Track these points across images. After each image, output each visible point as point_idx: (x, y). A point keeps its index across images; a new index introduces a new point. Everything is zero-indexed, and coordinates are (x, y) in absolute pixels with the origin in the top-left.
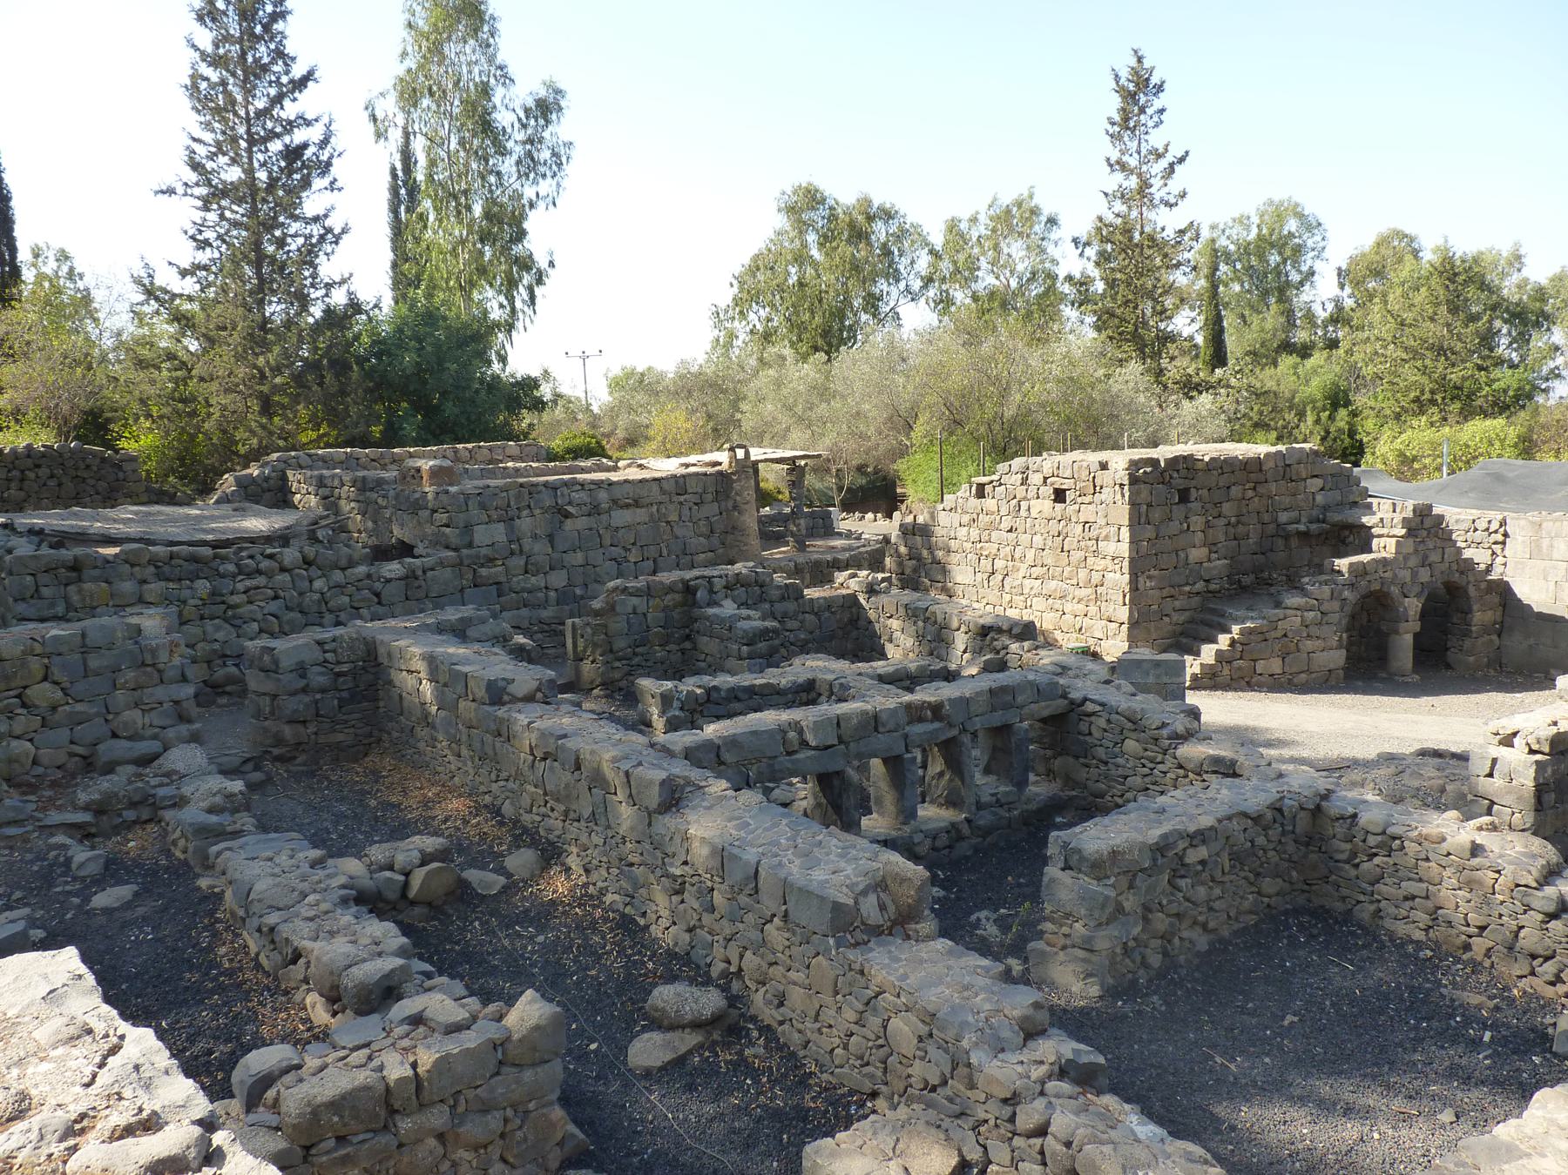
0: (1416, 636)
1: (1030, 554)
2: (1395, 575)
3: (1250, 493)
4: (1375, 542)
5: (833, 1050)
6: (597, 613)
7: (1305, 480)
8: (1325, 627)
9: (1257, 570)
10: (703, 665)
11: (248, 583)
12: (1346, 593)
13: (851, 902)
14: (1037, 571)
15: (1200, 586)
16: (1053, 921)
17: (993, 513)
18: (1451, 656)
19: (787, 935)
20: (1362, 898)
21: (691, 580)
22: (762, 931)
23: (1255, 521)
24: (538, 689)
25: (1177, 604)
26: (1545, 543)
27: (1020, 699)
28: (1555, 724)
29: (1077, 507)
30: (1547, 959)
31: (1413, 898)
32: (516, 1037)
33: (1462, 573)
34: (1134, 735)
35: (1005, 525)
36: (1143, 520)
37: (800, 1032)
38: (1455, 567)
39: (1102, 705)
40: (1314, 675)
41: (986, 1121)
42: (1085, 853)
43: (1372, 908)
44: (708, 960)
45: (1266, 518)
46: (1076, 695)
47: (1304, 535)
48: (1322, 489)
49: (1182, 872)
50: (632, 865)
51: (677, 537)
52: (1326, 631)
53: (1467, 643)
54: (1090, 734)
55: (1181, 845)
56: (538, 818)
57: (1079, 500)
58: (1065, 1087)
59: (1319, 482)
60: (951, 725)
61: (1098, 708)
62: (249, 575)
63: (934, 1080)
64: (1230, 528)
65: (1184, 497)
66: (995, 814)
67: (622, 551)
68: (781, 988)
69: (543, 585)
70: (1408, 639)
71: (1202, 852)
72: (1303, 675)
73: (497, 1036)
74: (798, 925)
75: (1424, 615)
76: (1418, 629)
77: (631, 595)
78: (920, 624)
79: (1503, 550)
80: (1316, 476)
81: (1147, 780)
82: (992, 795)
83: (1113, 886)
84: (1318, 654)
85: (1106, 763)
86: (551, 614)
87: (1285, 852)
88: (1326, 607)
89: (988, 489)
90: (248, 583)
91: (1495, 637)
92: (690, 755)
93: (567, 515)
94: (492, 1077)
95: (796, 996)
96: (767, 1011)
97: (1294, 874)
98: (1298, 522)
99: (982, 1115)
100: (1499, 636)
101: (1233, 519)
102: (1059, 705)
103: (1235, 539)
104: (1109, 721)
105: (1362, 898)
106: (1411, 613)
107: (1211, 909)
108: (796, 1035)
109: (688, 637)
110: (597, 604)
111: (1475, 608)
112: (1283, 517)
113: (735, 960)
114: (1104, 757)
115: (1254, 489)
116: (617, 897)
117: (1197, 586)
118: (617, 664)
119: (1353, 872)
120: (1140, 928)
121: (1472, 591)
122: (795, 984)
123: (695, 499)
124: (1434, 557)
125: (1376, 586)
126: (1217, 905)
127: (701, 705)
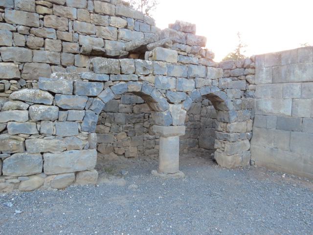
2: (157, 79)
4: (147, 53)
12: (94, 91)
18: (217, 155)
33: (223, 90)
38: (216, 83)
40: (50, 178)
45: (65, 36)
48: (126, 27)
52: (65, 128)
53: (228, 146)
59: (123, 22)
72: (35, 178)
76: (183, 133)
79: (254, 78)
80: (121, 16)
88: (62, 101)
91: (247, 142)
100: (250, 141)
103: (26, 46)
111: (233, 118)
115: (52, 7)
121: (231, 106)
125: (135, 87)
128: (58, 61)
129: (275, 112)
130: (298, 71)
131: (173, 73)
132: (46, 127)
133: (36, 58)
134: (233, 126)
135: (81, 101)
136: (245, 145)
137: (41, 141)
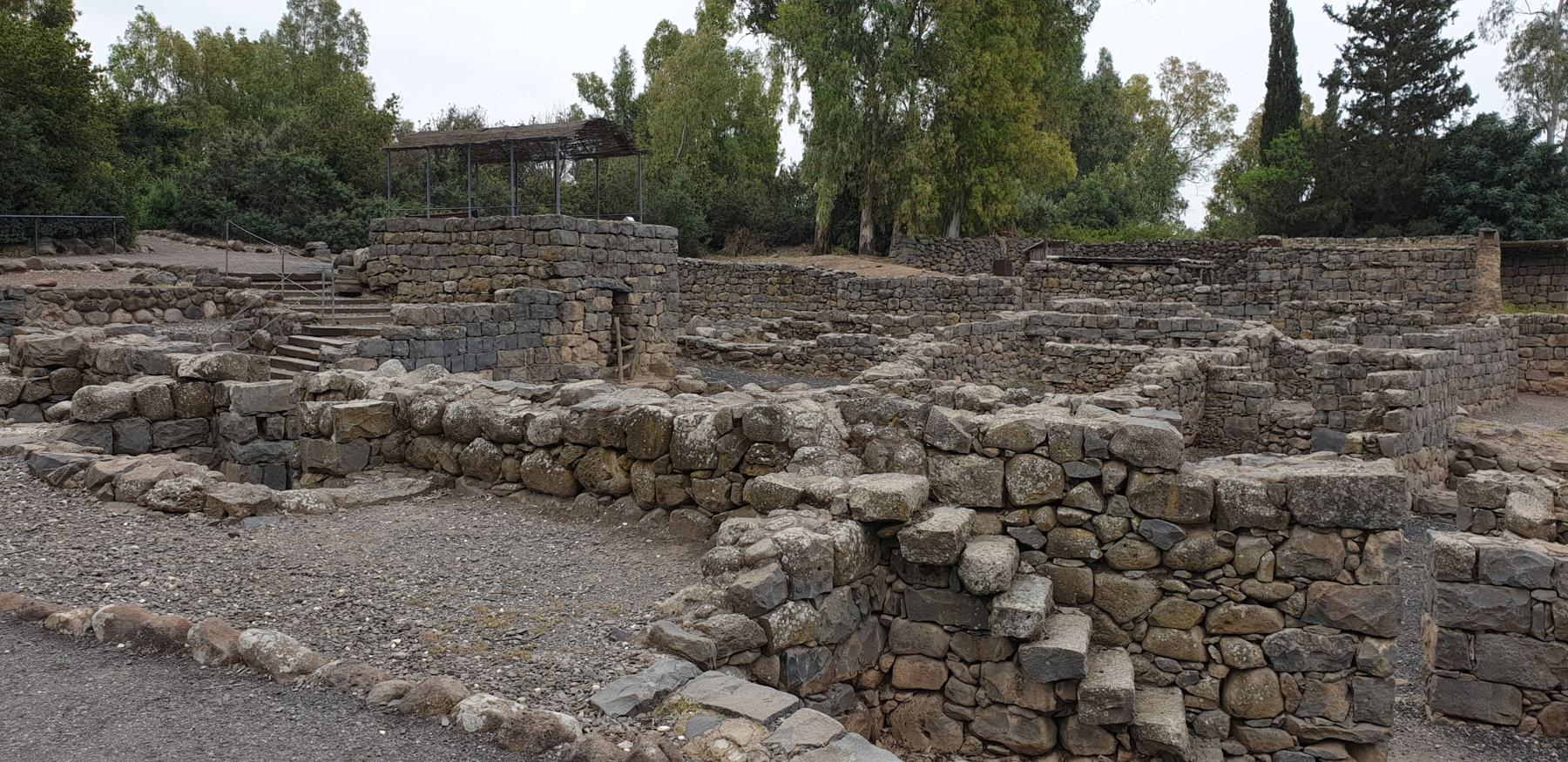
11: (1121, 286)
51: (1420, 290)
55: (1088, 353)
62: (1123, 282)
90: (1121, 286)
93: (1325, 269)
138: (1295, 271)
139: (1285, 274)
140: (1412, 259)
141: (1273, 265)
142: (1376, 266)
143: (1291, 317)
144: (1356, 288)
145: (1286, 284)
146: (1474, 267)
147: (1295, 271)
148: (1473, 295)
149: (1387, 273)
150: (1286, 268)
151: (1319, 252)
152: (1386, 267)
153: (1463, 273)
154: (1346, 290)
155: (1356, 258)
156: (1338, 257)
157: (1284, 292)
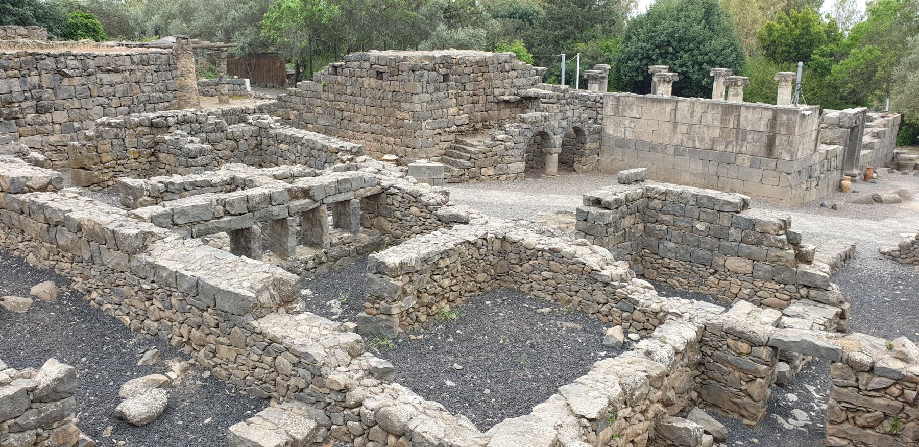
0: (560, 155)
1: (364, 109)
3: (480, 78)
5: (245, 377)
6: (89, 139)
7: (508, 72)
8: (515, 151)
9: (484, 120)
10: (163, 171)
13: (254, 295)
14: (367, 118)
15: (454, 128)
16: (369, 301)
17: (342, 84)
19: (216, 317)
20: (524, 281)
21: (154, 118)
22: (202, 316)
23: (482, 94)
24: (50, 183)
25: (442, 138)
26: (621, 108)
27: (354, 186)
28: (615, 194)
29: (389, 82)
30: (605, 304)
31: (547, 279)
32: (41, 387)
34: (414, 204)
35: (349, 92)
36: (424, 91)
37: (225, 369)
39: (399, 189)
41: (330, 403)
42: (387, 264)
43: (528, 286)
44: (170, 336)
45: (488, 91)
46: (385, 183)
47: (507, 102)
49: (437, 272)
50: (119, 285)
51: (143, 92)
53: (583, 159)
54: (393, 204)
55: (437, 258)
56: (53, 263)
57: (390, 79)
58: (373, 381)
59: (515, 73)
60: (315, 201)
61: (396, 191)
63: (301, 386)
64: (469, 97)
65: (446, 77)
66: (341, 248)
67: (106, 100)
68: (214, 347)
69: (50, 120)
70: (556, 156)
71: (448, 261)
73: (29, 386)
74: (223, 311)
75: (563, 145)
77: (113, 127)
78: (299, 146)
81: (422, 227)
82: (339, 239)
83: (401, 280)
84: (512, 164)
85: (401, 220)
86: (58, 140)
87: (488, 260)
89: (339, 70)
91: (596, 156)
92: (153, 219)
93: (65, 75)
94: (26, 410)
95: (223, 351)
96: (206, 361)
97: (492, 271)
98: (504, 94)
99: (328, 401)
101: (471, 93)
102: (375, 190)
104: (403, 197)
105: (524, 281)
106: (557, 143)
107: (451, 290)
108: (223, 372)
109: (153, 154)
110: (90, 133)
111: (587, 141)
112: (497, 92)
113: (185, 334)
114: (400, 217)
116: (109, 306)
117: (452, 128)
118: (105, 170)
119: (520, 269)
120: (415, 302)
121: (587, 133)
122: (222, 344)
123: (154, 68)
124: (569, 114)
125: (540, 129)
126: (454, 288)
127: (161, 193)
128: (484, 109)
129: (615, 135)
130: (628, 111)
131: (557, 118)
132: (510, 152)
133: (476, 109)
134: (588, 145)
135: (521, 139)
136: (594, 158)
137: (507, 158)
138: (34, 79)
139: (24, 82)
140: (133, 63)
141: (10, 73)
142: (109, 71)
143: (116, 137)
144: (96, 94)
145: (28, 95)
146: (176, 69)
147: (34, 79)
148: (178, 94)
149: (116, 78)
150: (23, 76)
151: (55, 57)
152: (117, 71)
153: (169, 74)
154: (86, 97)
155: (92, 63)
156: (75, 62)
157: (28, 103)
